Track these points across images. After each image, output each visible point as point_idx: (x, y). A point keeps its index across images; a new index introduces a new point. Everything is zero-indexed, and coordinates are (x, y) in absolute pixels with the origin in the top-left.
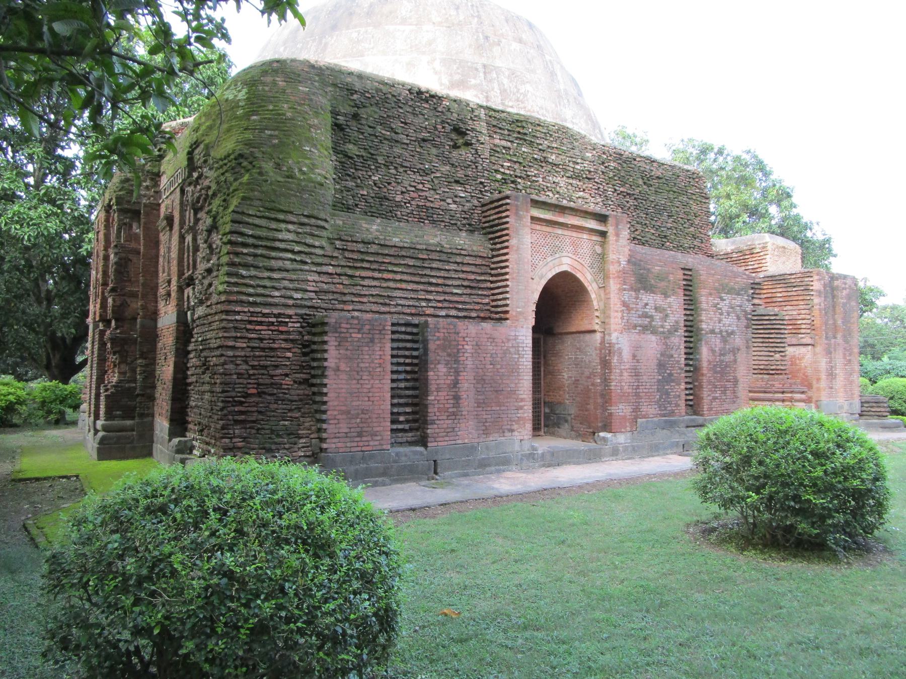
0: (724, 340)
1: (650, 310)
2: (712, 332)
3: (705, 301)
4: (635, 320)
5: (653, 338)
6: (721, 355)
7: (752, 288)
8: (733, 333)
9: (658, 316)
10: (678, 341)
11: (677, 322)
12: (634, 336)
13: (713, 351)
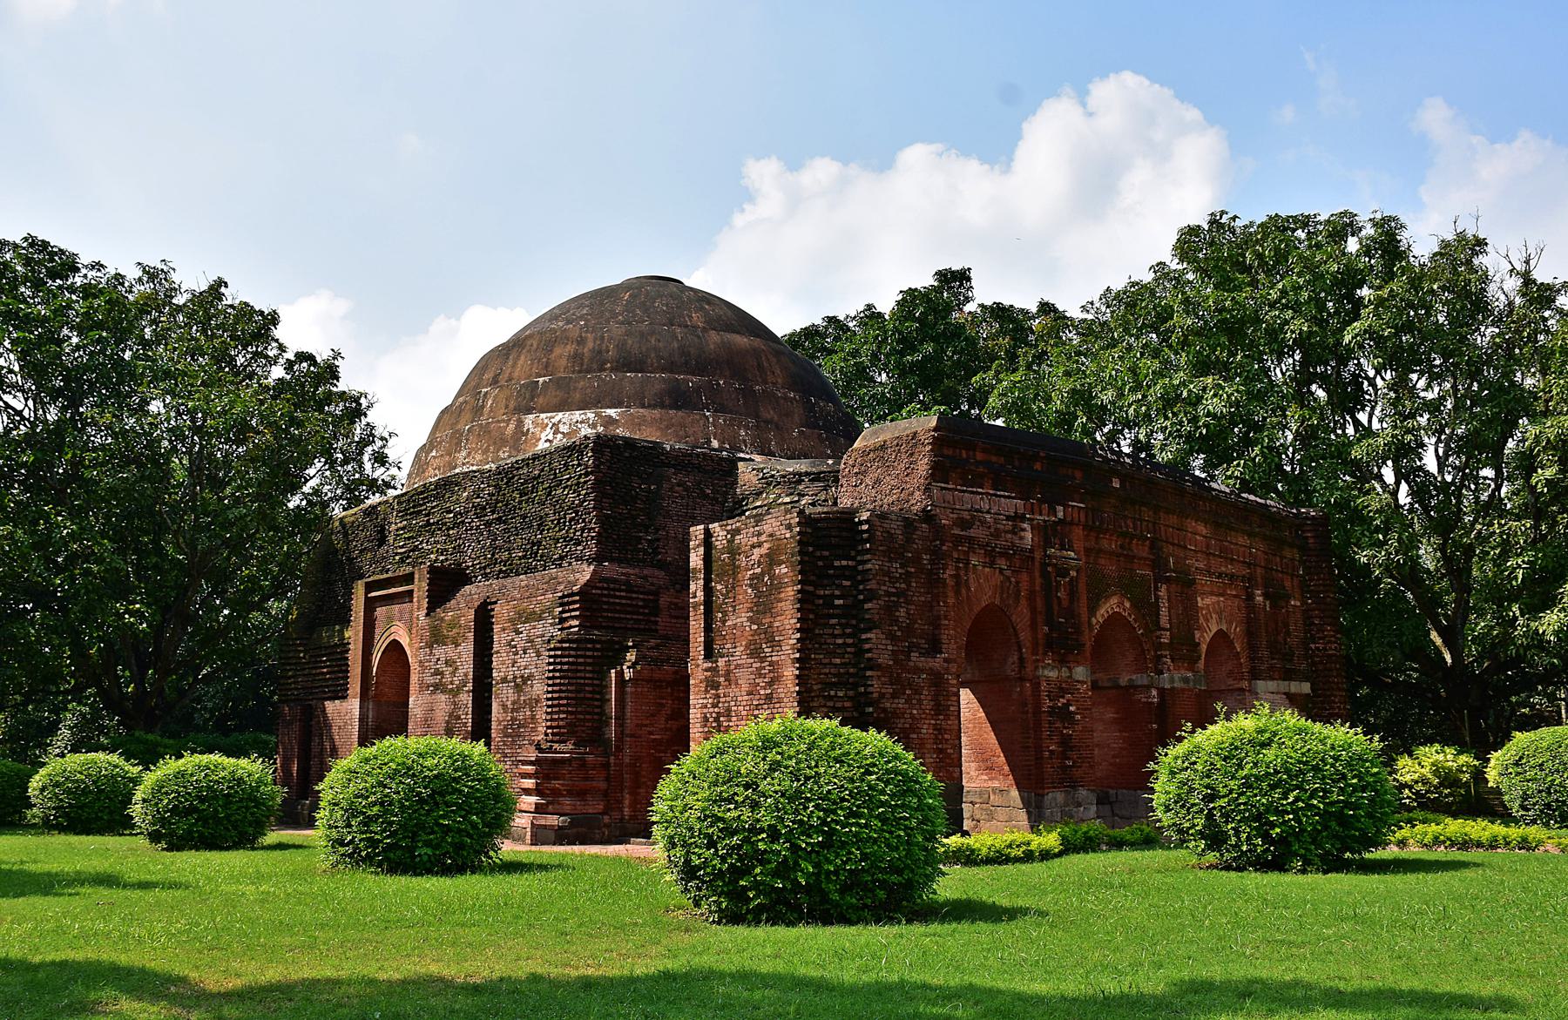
0: (518, 688)
1: (441, 666)
2: (504, 680)
3: (499, 638)
4: (430, 680)
5: (443, 697)
6: (513, 710)
7: (561, 605)
8: (531, 677)
9: (448, 670)
10: (466, 699)
11: (466, 675)
12: (427, 697)
13: (504, 706)
